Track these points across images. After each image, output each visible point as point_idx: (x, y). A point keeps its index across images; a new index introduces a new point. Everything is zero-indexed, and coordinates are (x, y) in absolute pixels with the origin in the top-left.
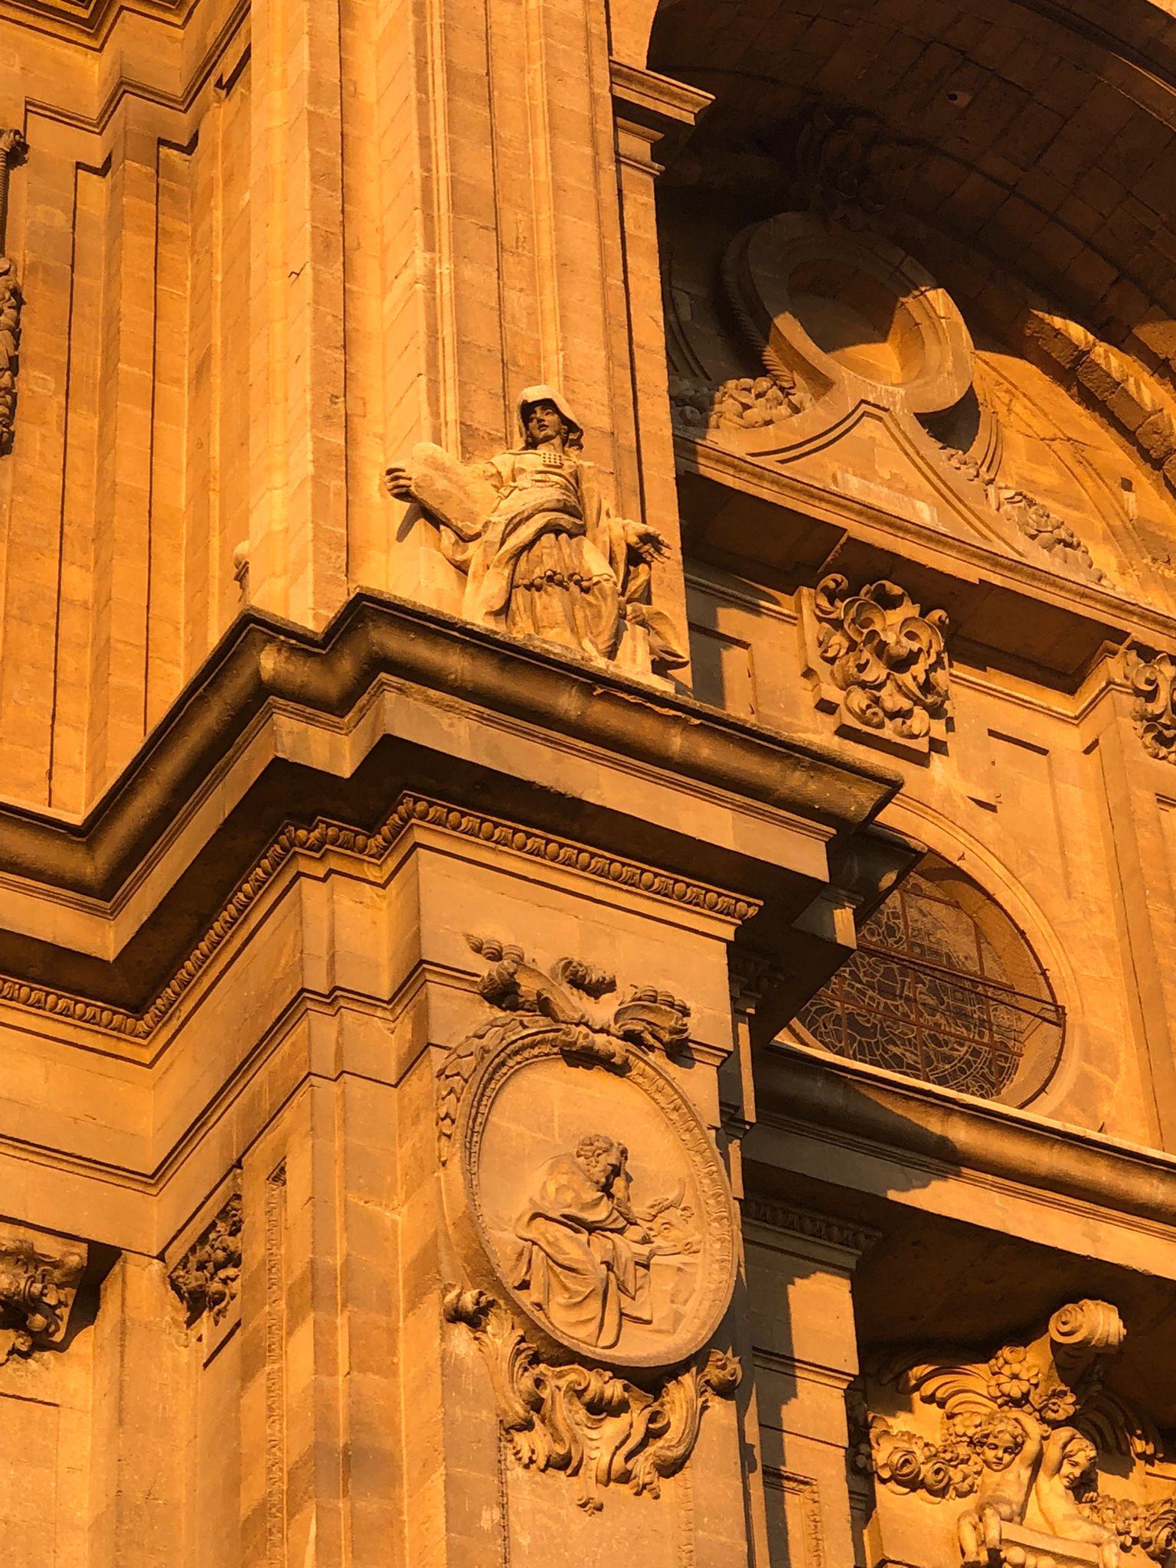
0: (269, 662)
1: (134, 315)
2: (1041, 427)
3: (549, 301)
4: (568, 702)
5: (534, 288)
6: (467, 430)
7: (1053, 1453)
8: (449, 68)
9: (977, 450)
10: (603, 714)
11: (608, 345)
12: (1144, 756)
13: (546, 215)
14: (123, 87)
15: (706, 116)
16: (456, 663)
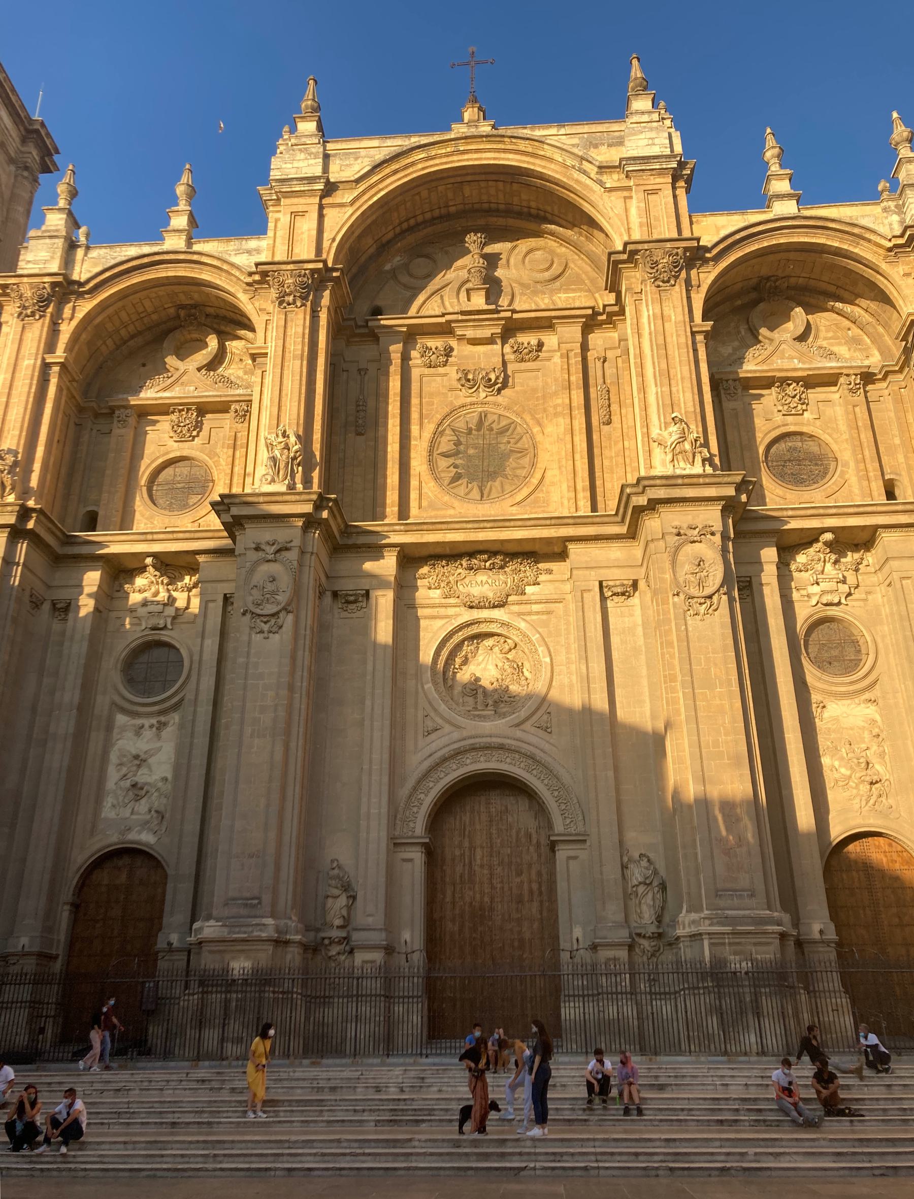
0: (628, 490)
1: (628, 388)
2: (827, 323)
3: (680, 387)
4: (680, 481)
5: (678, 385)
6: (665, 423)
7: (827, 559)
8: (657, 345)
9: (811, 339)
10: (687, 481)
11: (693, 394)
12: (850, 398)
13: (678, 369)
14: (620, 341)
15: (713, 327)
16: (658, 482)
